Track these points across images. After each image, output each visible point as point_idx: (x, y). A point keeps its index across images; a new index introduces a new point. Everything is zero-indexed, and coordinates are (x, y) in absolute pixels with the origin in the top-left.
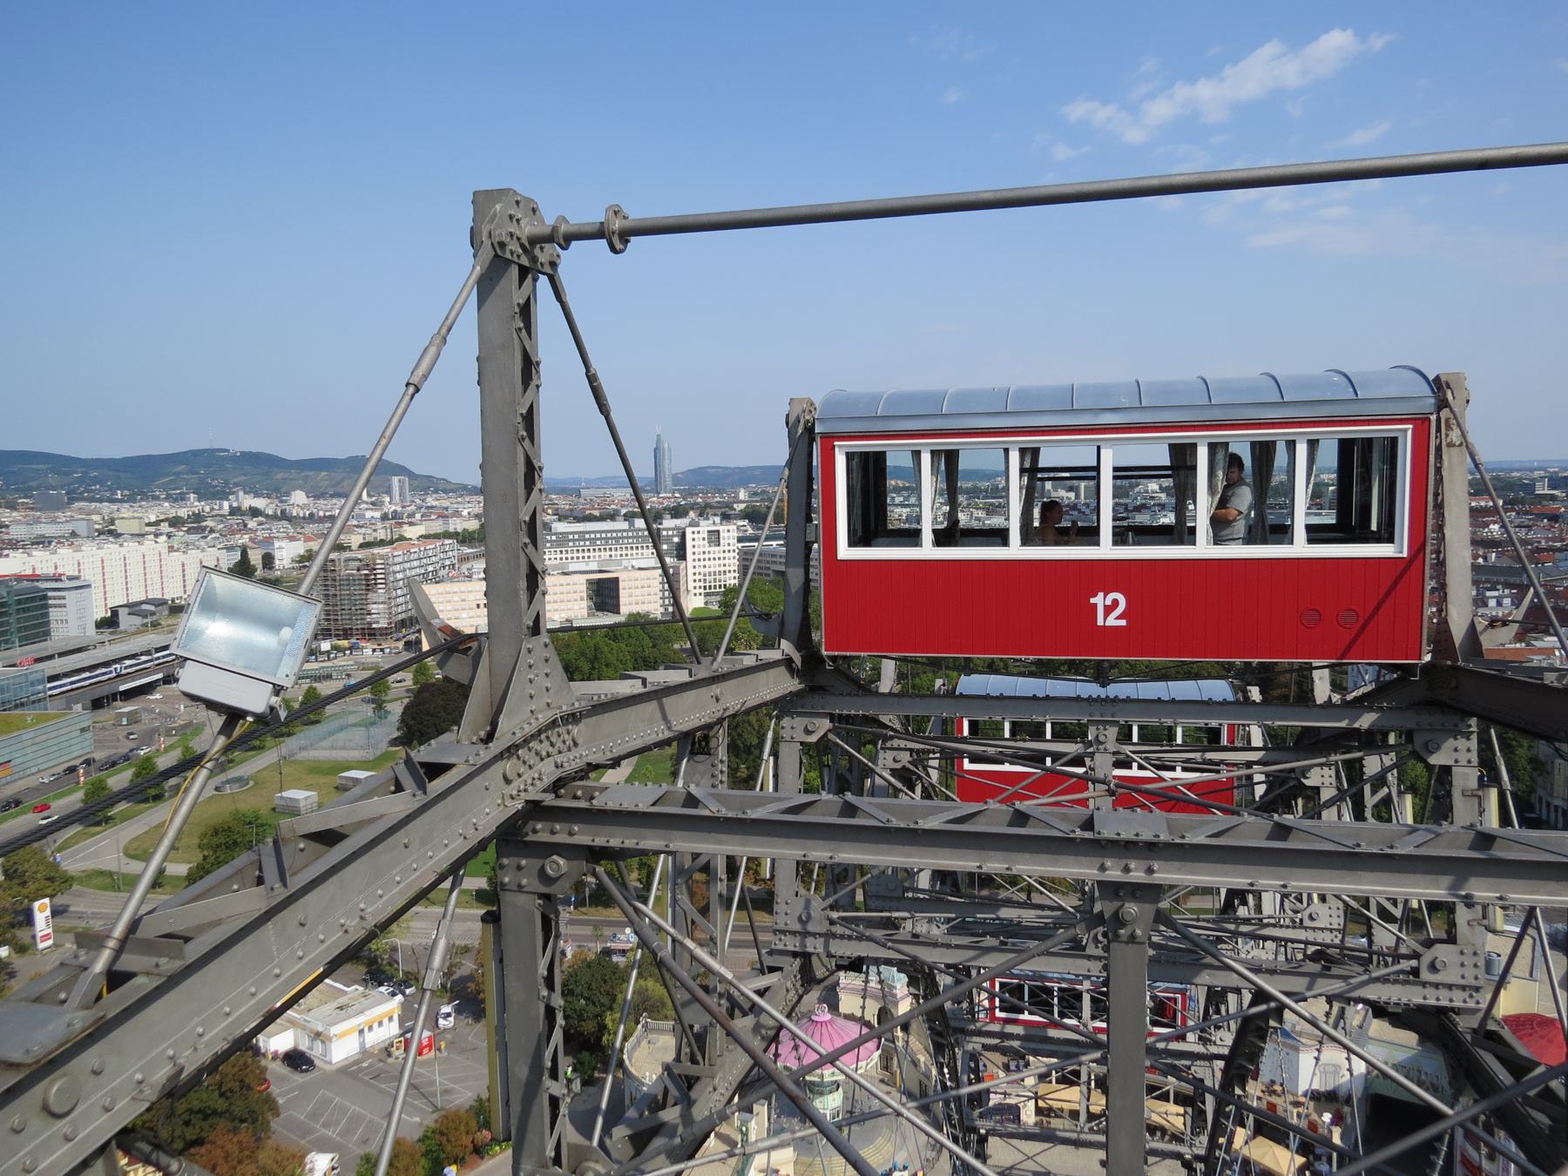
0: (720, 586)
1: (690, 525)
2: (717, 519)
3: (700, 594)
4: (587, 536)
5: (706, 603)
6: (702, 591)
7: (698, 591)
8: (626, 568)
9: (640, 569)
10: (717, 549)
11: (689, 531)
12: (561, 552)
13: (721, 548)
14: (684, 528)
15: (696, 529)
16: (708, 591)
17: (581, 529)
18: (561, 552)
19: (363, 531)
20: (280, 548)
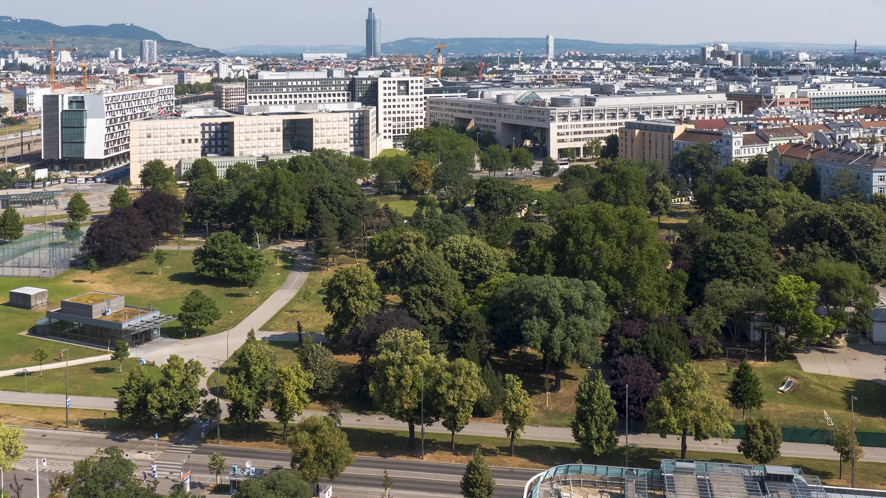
0: (403, 130)
1: (382, 76)
2: (407, 72)
3: (390, 137)
4: (290, 83)
5: (395, 146)
6: (391, 134)
7: (387, 134)
8: (321, 111)
9: (333, 112)
10: (406, 97)
11: (381, 81)
12: (271, 97)
13: (410, 97)
14: (377, 79)
15: (387, 79)
16: (397, 134)
17: (284, 77)
18: (271, 97)
19: (107, 81)
20: (32, 93)
